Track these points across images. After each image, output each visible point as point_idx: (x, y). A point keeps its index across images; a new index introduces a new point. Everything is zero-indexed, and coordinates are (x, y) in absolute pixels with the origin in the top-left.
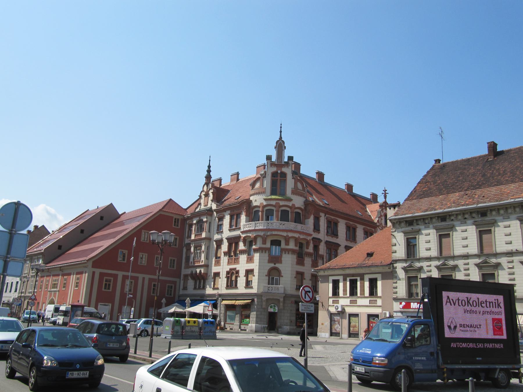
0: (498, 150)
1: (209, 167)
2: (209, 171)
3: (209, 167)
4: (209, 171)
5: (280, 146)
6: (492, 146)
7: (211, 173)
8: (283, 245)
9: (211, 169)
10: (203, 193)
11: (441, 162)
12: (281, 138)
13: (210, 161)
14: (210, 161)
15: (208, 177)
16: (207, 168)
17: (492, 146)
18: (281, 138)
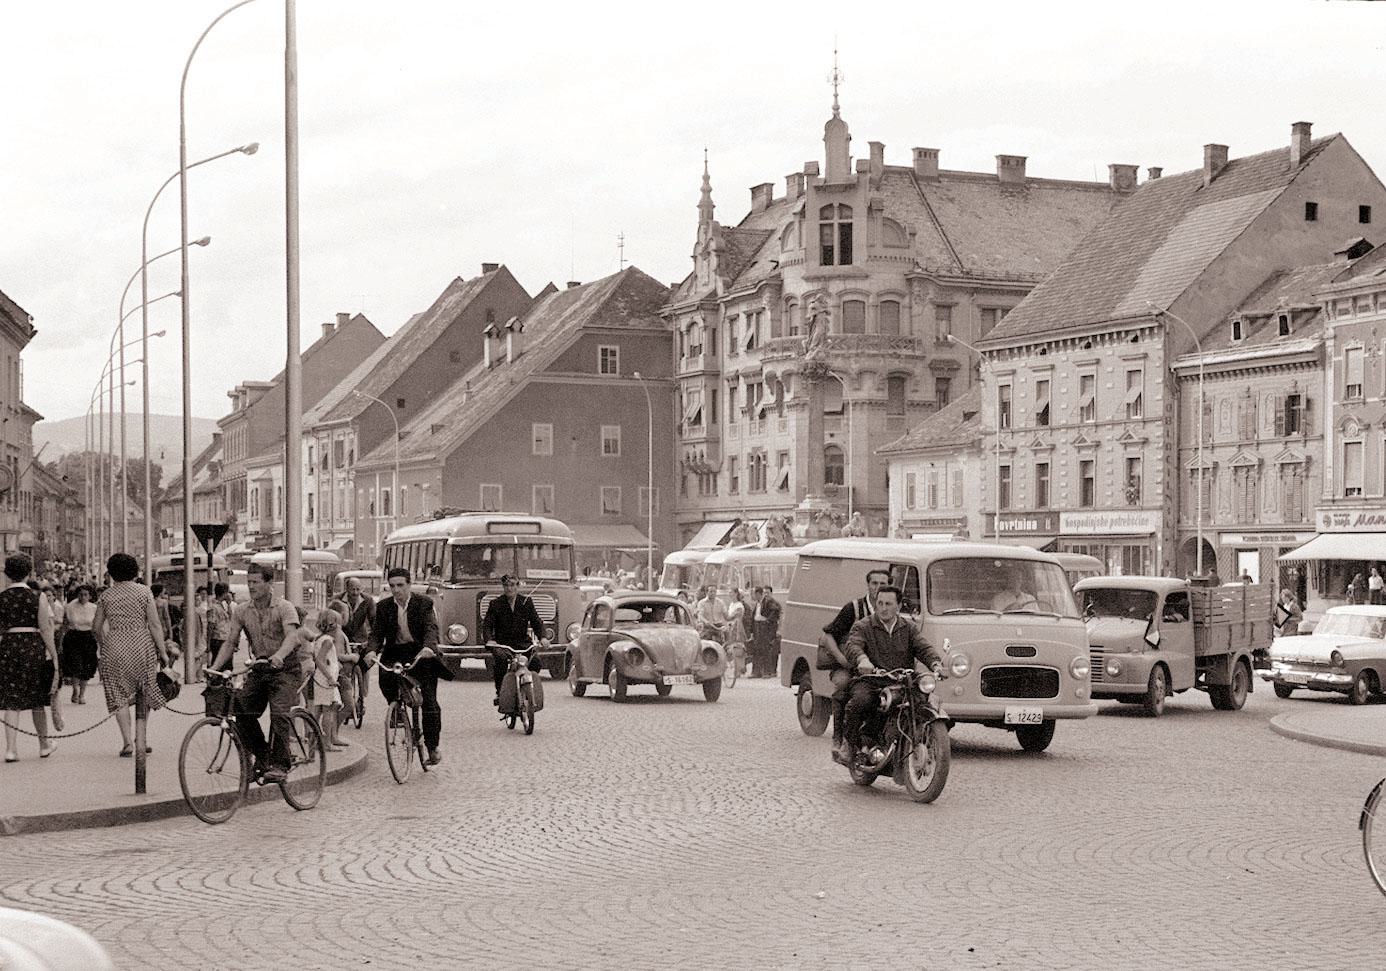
0: (1229, 159)
1: (706, 178)
2: (707, 190)
3: (706, 178)
4: (707, 190)
5: (836, 131)
6: (1217, 152)
7: (712, 195)
8: (849, 395)
9: (712, 183)
10: (700, 249)
11: (1164, 174)
12: (836, 108)
13: (706, 162)
14: (706, 162)
15: (707, 207)
16: (701, 183)
17: (1217, 152)
18: (836, 108)
